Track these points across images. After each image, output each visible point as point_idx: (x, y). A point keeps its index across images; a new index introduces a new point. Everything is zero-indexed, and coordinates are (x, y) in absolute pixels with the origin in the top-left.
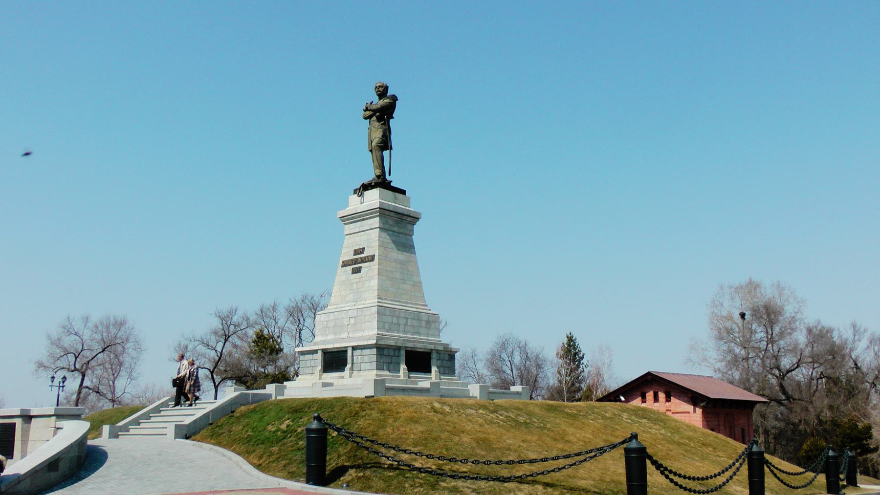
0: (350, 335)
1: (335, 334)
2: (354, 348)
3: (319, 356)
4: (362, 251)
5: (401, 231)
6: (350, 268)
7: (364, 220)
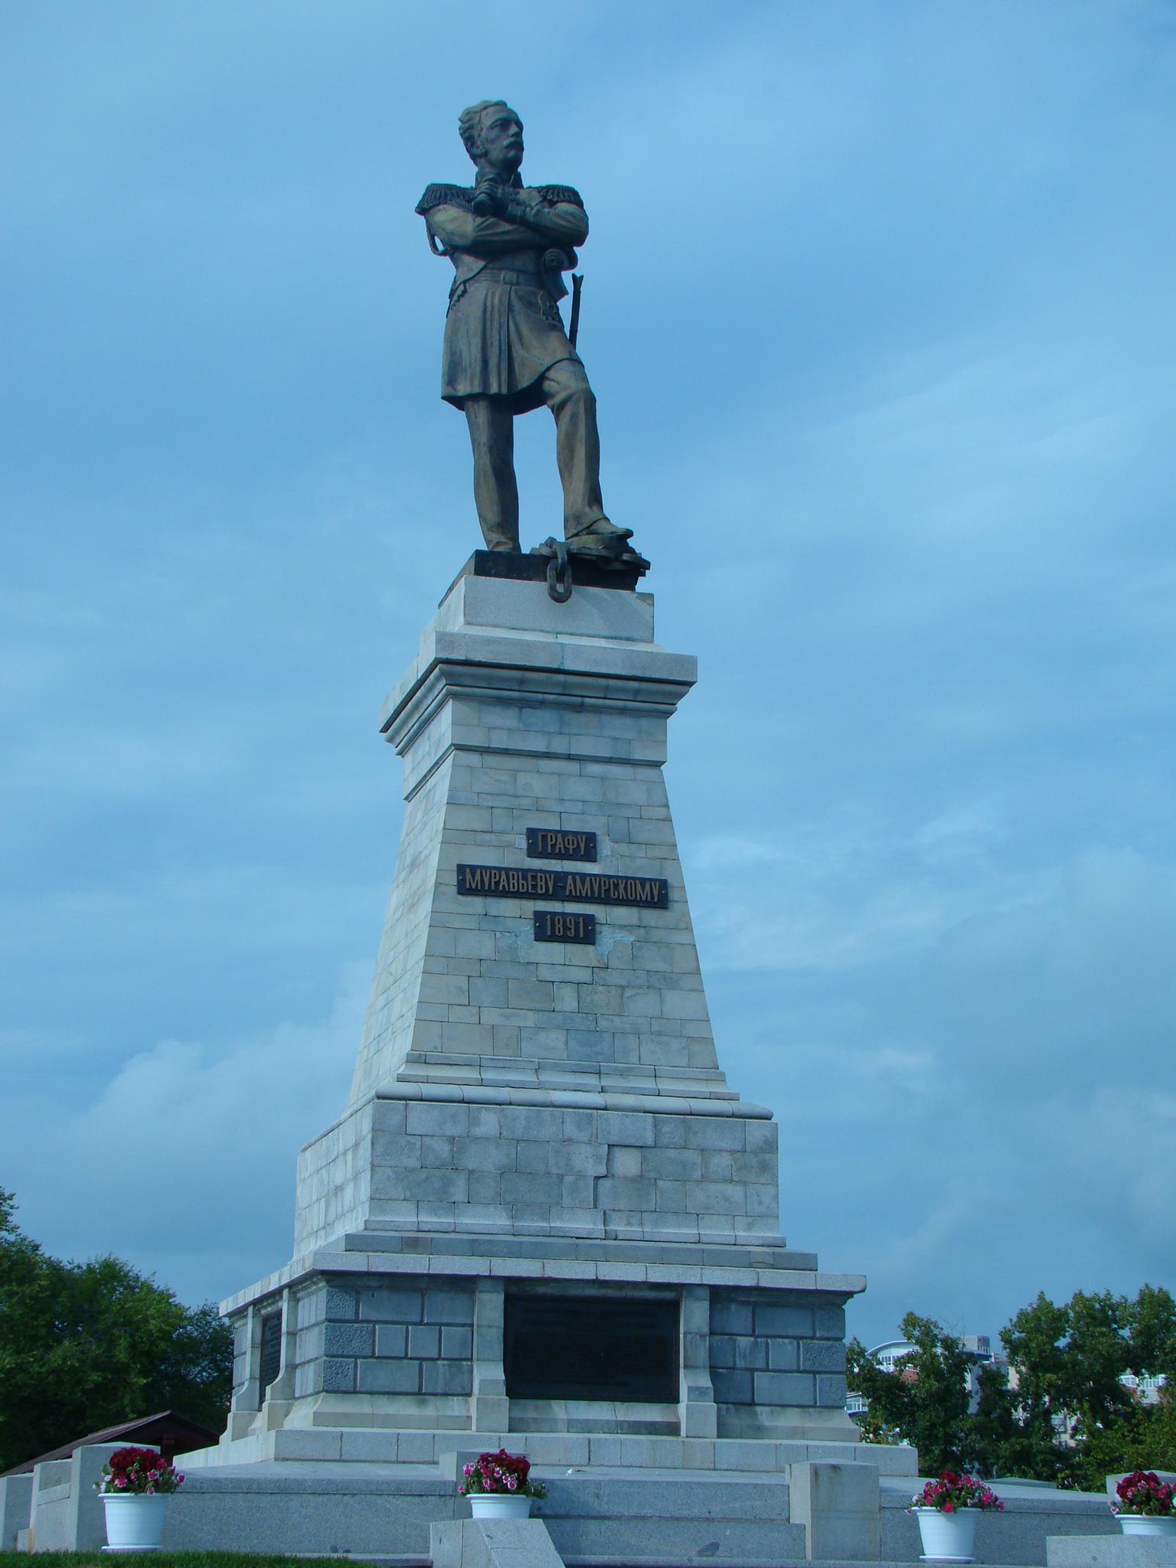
0: (618, 1226)
1: (514, 1209)
2: (720, 1296)
3: (490, 1309)
4: (586, 846)
6: (517, 912)
7: (580, 708)
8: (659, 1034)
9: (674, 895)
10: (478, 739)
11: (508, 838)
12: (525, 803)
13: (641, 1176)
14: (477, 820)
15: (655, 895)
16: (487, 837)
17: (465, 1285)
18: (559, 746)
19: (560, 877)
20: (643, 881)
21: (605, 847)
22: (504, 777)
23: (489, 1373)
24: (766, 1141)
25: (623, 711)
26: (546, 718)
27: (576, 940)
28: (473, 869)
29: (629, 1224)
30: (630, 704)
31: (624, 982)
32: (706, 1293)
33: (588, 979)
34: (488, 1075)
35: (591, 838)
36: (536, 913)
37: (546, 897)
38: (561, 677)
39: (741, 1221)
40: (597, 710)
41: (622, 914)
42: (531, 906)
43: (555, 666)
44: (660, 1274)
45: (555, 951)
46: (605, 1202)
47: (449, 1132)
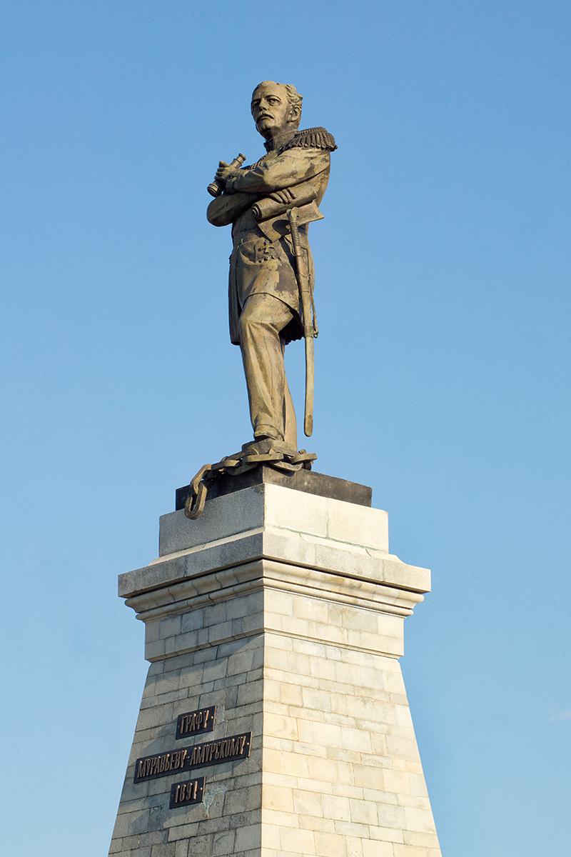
5: (353, 640)
6: (162, 786)
7: (212, 603)
10: (159, 652)
21: (220, 717)
25: (237, 595)
37: (179, 770)
40: (223, 600)
41: (223, 771)
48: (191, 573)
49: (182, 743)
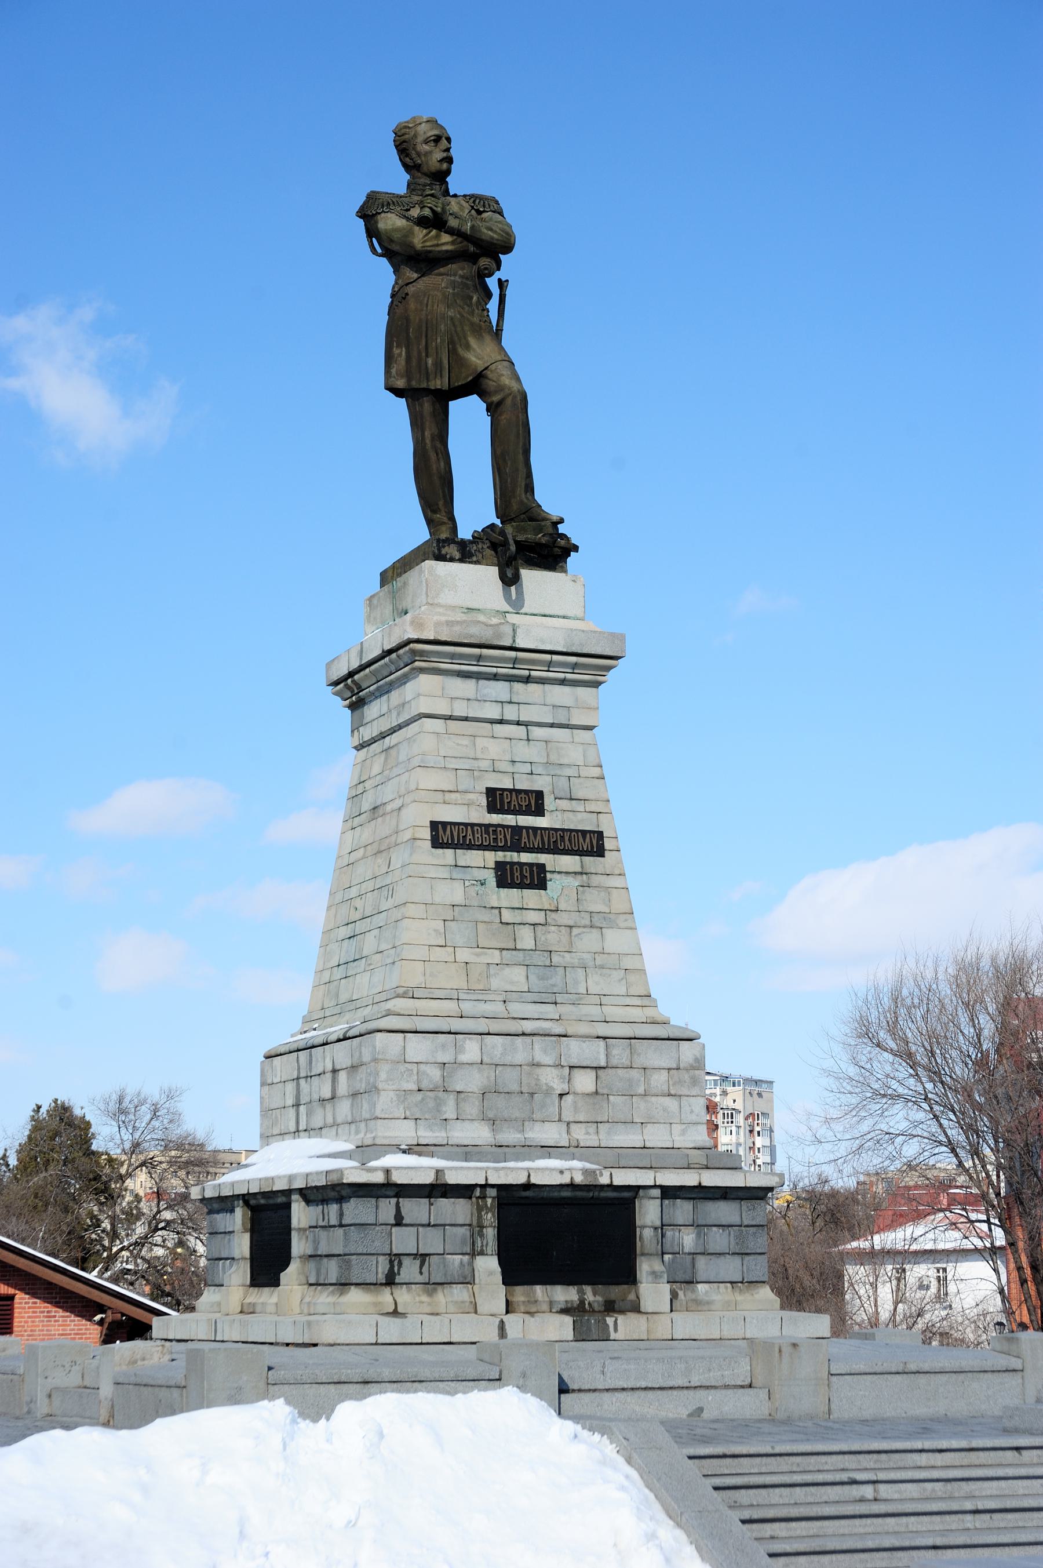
0: (580, 1134)
2: (669, 1193)
4: (535, 803)
7: (527, 680)
8: (602, 967)
9: (608, 844)
11: (471, 796)
12: (485, 765)
13: (597, 1093)
14: (445, 781)
15: (591, 844)
16: (454, 796)
17: (463, 1191)
18: (510, 713)
19: (517, 830)
20: (584, 833)
21: (549, 802)
22: (465, 741)
23: (489, 1265)
24: (697, 1060)
25: (563, 682)
26: (499, 689)
27: (531, 886)
28: (444, 824)
29: (588, 1133)
30: (569, 676)
31: (571, 923)
32: (657, 1192)
33: (543, 921)
34: (467, 1007)
35: (539, 795)
36: (497, 863)
37: (503, 849)
38: (513, 654)
39: (677, 1129)
41: (569, 862)
42: (491, 858)
43: (508, 643)
44: (623, 1178)
45: (511, 896)
46: (567, 1116)
47: (440, 1060)
48: (521, 643)
49: (496, 819)
